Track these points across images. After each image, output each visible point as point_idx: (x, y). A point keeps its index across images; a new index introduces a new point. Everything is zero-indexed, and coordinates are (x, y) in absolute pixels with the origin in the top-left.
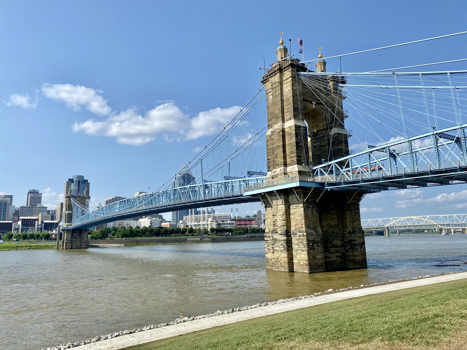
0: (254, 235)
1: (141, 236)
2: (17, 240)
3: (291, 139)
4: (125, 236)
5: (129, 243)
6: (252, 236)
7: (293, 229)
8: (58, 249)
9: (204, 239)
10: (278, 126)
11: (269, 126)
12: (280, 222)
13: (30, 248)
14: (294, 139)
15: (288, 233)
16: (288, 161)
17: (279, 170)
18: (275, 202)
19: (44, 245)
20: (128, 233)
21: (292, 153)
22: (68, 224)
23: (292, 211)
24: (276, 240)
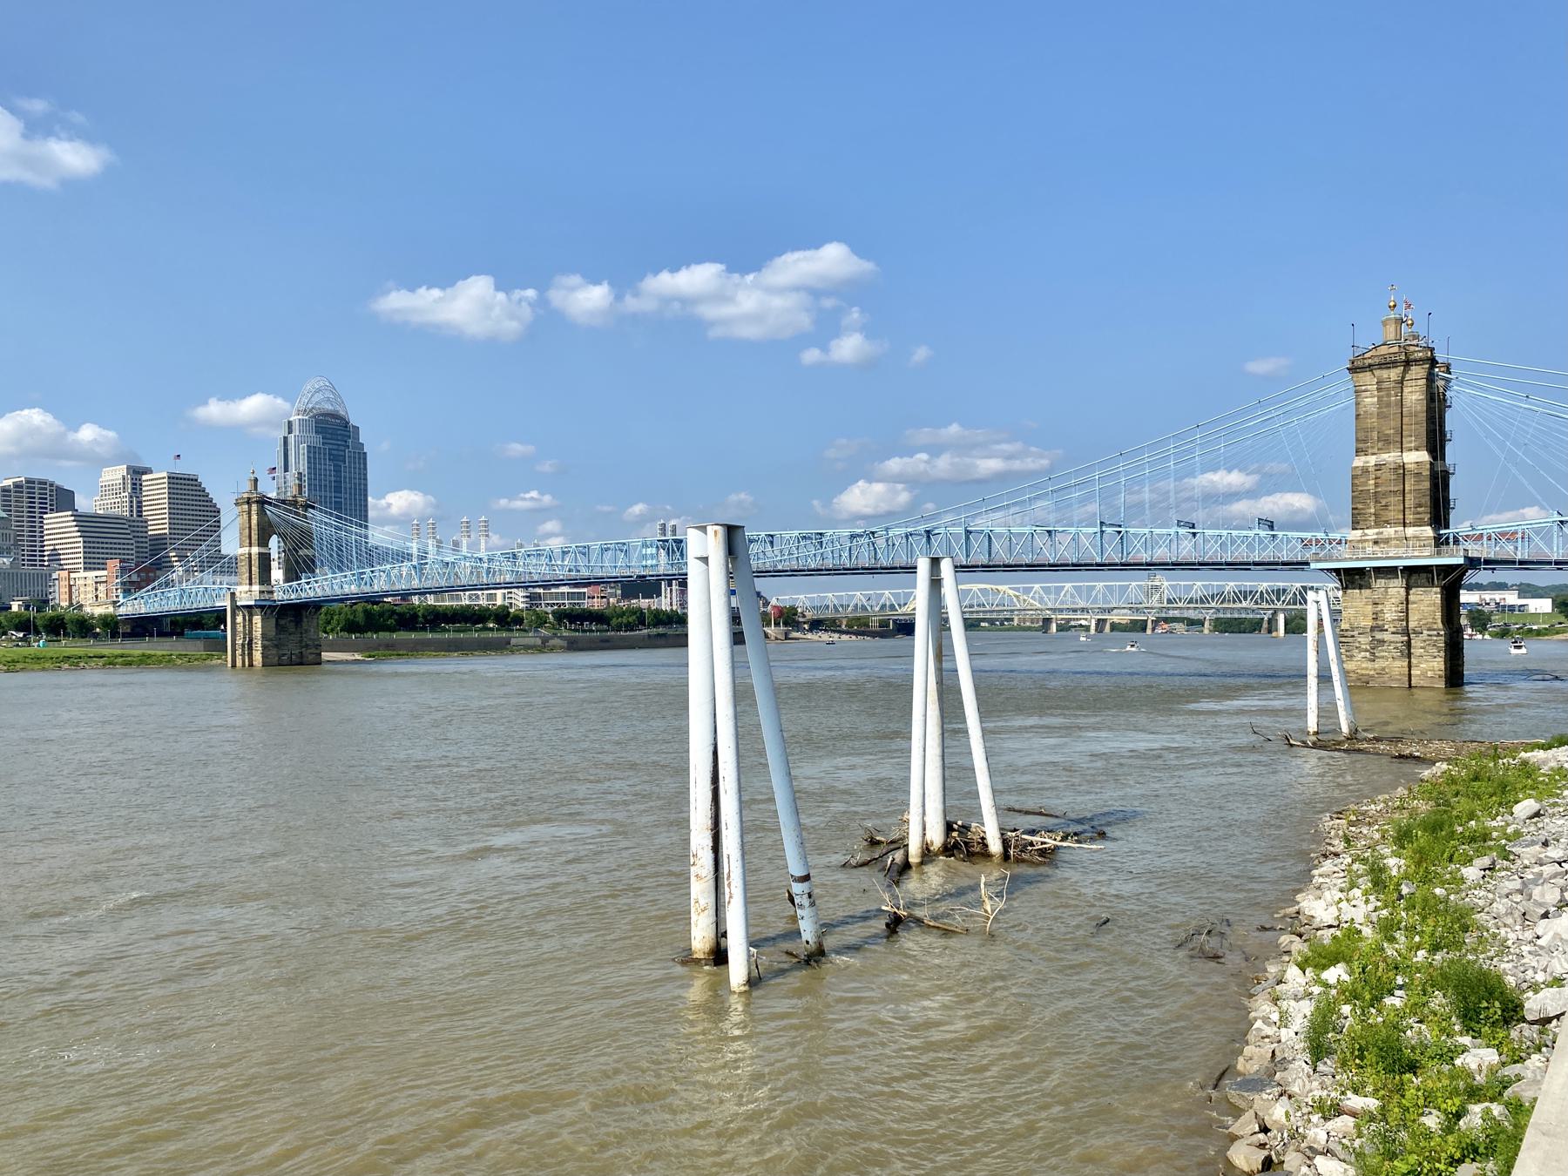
0: (661, 630)
1: (392, 630)
2: (23, 639)
3: (1418, 482)
4: (351, 627)
5: (367, 649)
6: (659, 635)
7: (1412, 625)
8: (234, 666)
9: (552, 642)
10: (1390, 457)
11: (1358, 452)
12: (1390, 613)
13: (110, 663)
14: (1427, 485)
15: (1406, 632)
16: (1410, 518)
17: (1389, 531)
18: (1381, 582)
19: (138, 652)
20: (360, 618)
21: (1420, 506)
22: (264, 588)
23: (1411, 598)
24: (1382, 642)
